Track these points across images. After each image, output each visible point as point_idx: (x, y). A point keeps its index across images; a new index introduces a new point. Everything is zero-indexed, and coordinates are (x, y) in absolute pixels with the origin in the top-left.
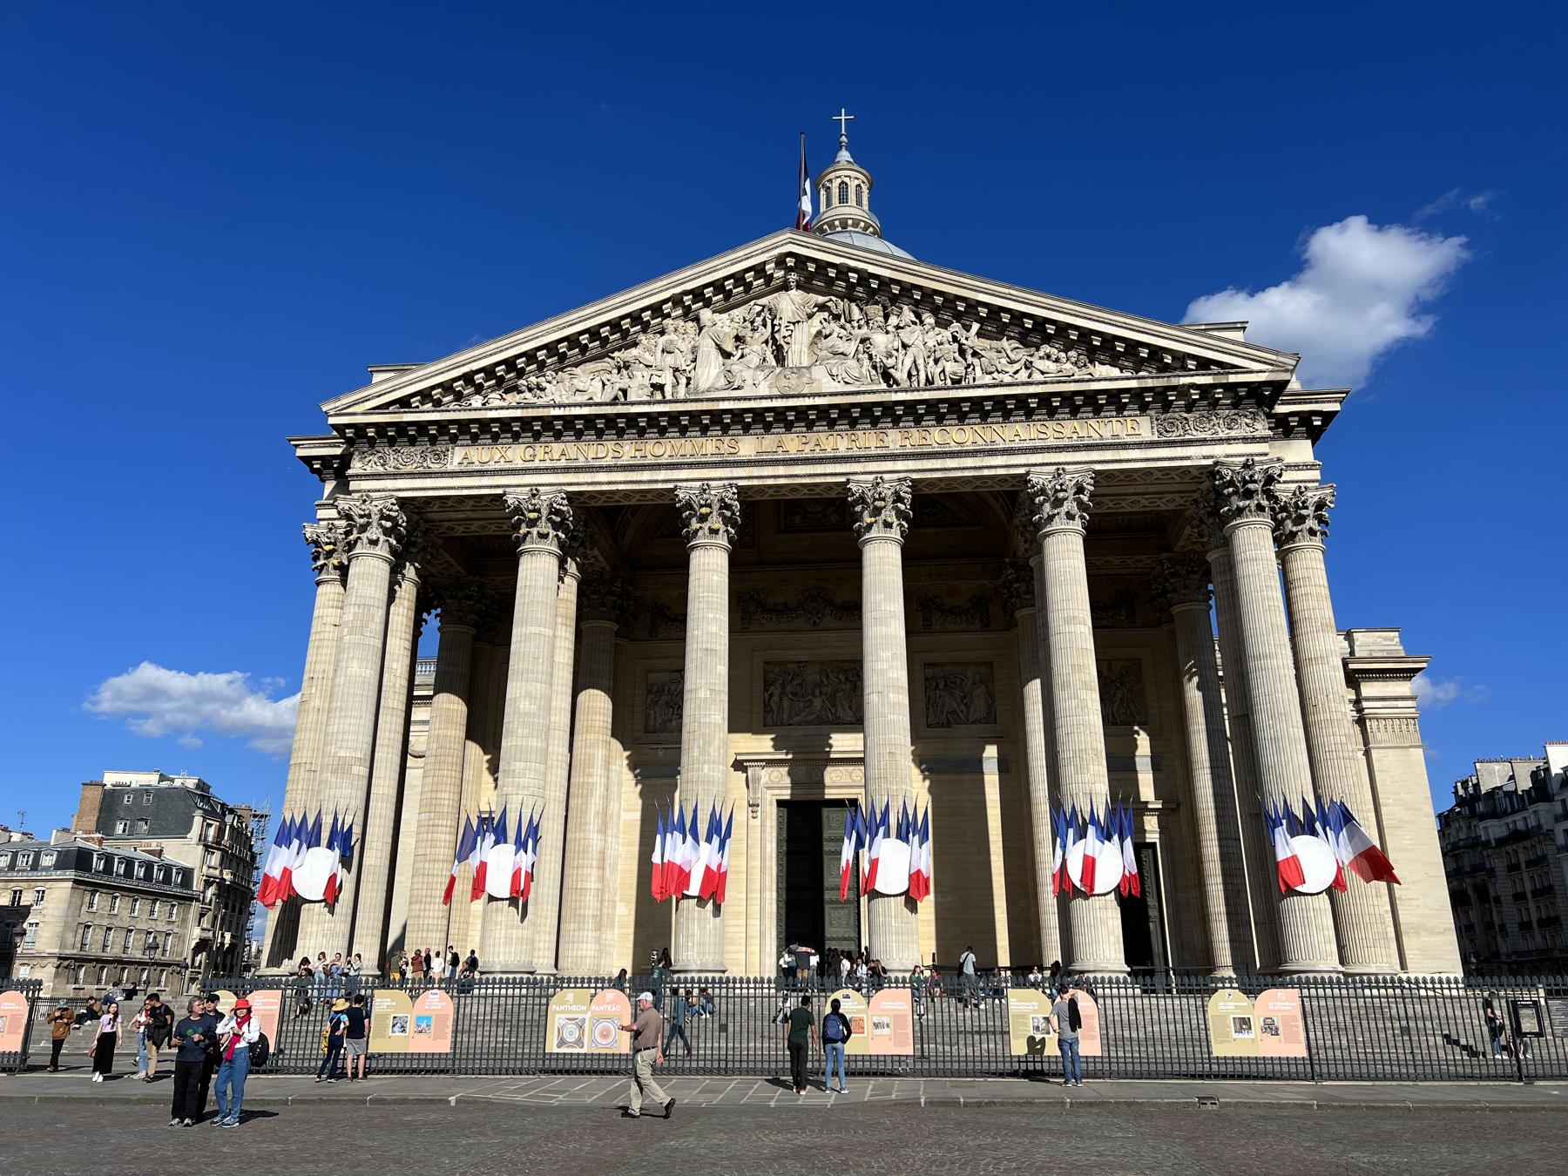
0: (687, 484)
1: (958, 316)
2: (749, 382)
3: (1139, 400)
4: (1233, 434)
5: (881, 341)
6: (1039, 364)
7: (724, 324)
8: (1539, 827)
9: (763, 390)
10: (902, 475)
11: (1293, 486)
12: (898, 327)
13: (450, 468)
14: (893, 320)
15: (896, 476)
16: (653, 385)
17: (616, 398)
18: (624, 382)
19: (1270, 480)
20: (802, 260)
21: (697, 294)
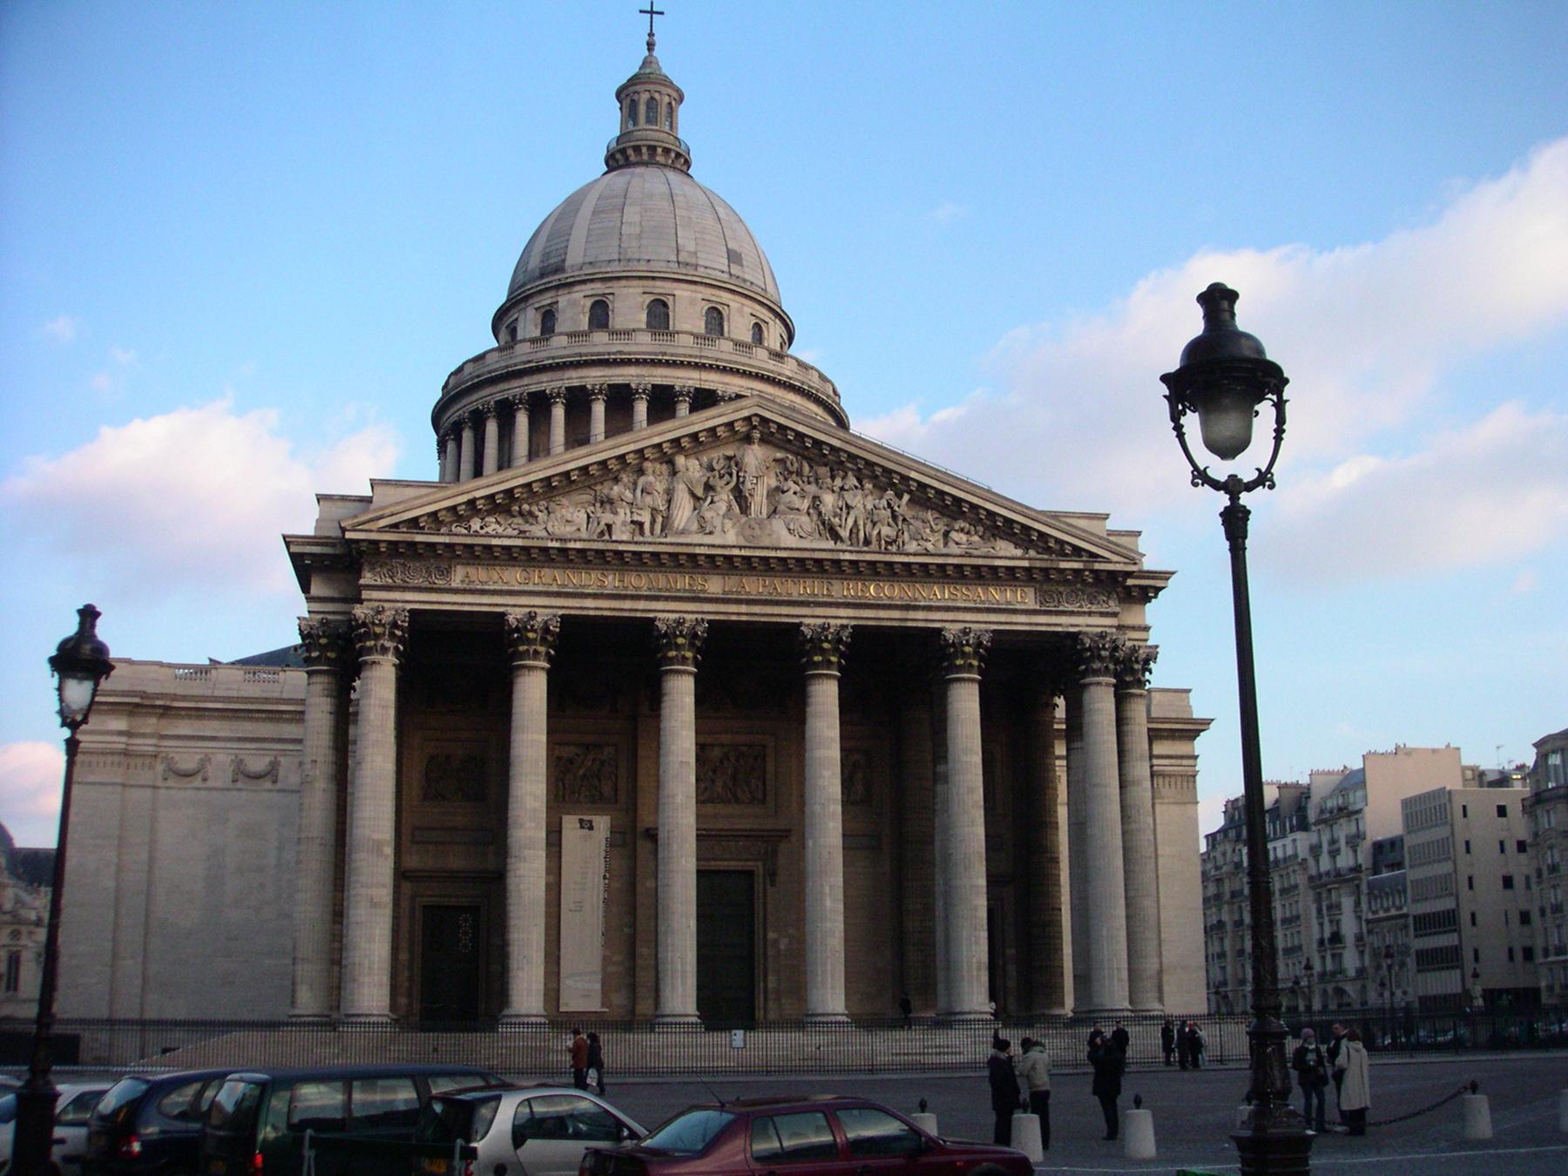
0: (665, 613)
1: (893, 486)
2: (719, 528)
3: (1027, 577)
4: (1094, 608)
5: (829, 500)
6: (953, 535)
7: (691, 468)
8: (1296, 856)
9: (731, 537)
10: (845, 622)
11: (1129, 644)
12: (842, 489)
13: (454, 585)
14: (838, 482)
15: (839, 622)
16: (632, 522)
17: (602, 533)
18: (607, 518)
19: (1116, 648)
20: (764, 421)
21: (676, 442)
